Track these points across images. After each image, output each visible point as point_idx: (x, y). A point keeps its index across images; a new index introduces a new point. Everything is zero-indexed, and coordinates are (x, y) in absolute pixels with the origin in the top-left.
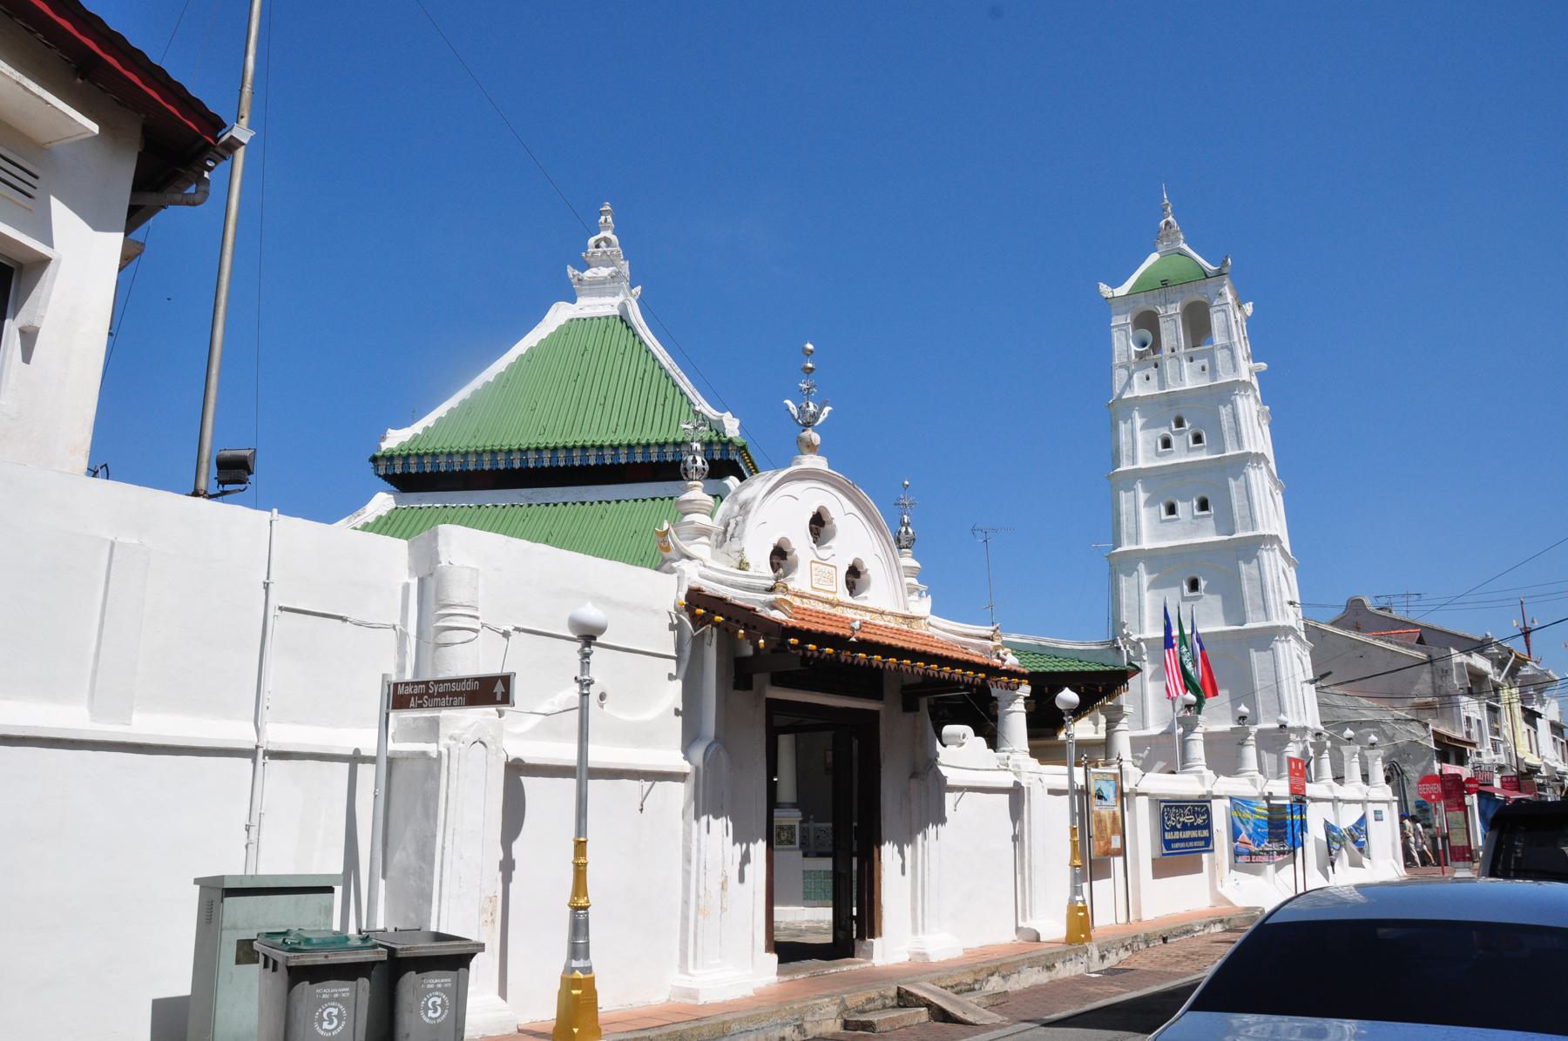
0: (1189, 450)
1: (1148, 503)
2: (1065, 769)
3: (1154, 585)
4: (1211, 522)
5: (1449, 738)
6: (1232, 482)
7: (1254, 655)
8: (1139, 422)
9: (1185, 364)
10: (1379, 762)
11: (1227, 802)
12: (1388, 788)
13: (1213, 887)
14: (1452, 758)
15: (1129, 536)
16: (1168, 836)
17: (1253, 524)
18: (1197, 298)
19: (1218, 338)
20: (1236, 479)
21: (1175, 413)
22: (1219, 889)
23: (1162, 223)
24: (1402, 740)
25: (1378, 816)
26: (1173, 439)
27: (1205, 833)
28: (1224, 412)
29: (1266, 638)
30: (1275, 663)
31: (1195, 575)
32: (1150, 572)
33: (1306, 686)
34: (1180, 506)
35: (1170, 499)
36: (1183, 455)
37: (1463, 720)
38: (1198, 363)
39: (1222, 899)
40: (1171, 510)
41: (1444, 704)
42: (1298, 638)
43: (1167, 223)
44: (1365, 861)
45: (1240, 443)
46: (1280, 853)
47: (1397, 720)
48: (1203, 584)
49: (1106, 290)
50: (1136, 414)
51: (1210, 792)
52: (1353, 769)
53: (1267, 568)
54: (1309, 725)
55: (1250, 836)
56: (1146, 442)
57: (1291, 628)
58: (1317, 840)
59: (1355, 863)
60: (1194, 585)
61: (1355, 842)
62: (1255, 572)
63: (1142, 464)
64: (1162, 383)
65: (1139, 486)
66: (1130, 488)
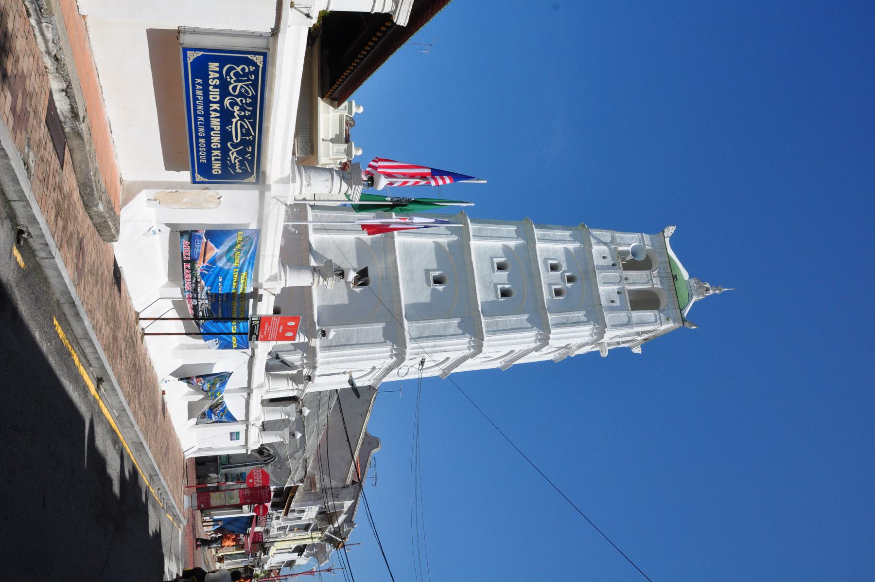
0: (550, 285)
1: (506, 249)
3: (438, 247)
4: (492, 298)
5: (293, 497)
6: (525, 317)
7: (380, 326)
8: (571, 246)
9: (616, 288)
10: (279, 440)
11: (253, 226)
12: (257, 447)
13: (148, 185)
14: (277, 500)
15: (480, 230)
16: (214, 66)
18: (664, 303)
19: (636, 315)
20: (528, 320)
21: (579, 275)
22: (143, 195)
23: (707, 285)
24: (291, 464)
25: (234, 436)
26: (557, 274)
27: (217, 167)
28: (581, 315)
29: (395, 337)
30: (373, 344)
31: (448, 282)
32: (450, 244)
33: (347, 377)
34: (504, 274)
35: (510, 266)
36: (546, 278)
37: (303, 508)
38: (616, 297)
39: (131, 192)
40: (501, 267)
41: (314, 494)
42: (389, 369)
43: (708, 289)
44: (194, 421)
45: (559, 325)
46: (195, 308)
47: (306, 461)
48: (440, 288)
50: (577, 245)
51: (268, 188)
52: (276, 414)
53: (455, 341)
55: (213, 262)
56: (555, 251)
57: (403, 360)
58: (212, 365)
59: (191, 407)
60: (438, 281)
61: (212, 409)
62: (451, 331)
63: (539, 246)
64: (603, 268)
65: (521, 242)
66: (519, 234)
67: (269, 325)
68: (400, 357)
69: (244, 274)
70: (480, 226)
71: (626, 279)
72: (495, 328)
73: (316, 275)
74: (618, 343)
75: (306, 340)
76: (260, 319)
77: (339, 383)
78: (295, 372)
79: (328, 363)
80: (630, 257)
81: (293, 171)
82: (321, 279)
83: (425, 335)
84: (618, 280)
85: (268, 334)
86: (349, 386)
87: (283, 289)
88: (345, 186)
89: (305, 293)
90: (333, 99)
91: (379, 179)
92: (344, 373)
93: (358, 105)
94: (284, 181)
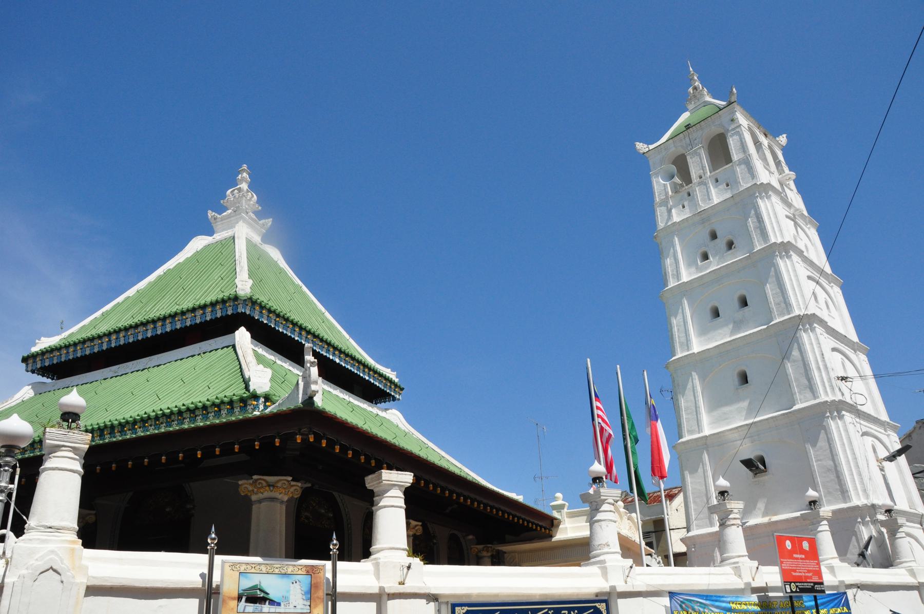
2: (204, 558)
11: (666, 601)
15: (681, 344)
17: (788, 306)
19: (736, 156)
33: (887, 464)
43: (695, 88)
49: (641, 147)
54: (876, 502)
63: (685, 277)
67: (795, 571)
68: (839, 408)
69: (733, 606)
70: (677, 346)
71: (701, 177)
72: (783, 305)
73: (728, 523)
74: (778, 164)
75: (825, 522)
76: (786, 582)
77: (900, 471)
78: (884, 530)
79: (865, 491)
80: (677, 180)
81: (594, 563)
82: (731, 516)
83: (806, 382)
84: (703, 187)
85: (809, 571)
86: (902, 459)
87: (752, 557)
88: (605, 507)
89: (750, 534)
90: (552, 525)
91: (594, 472)
92: (882, 470)
93: (555, 499)
94: (605, 572)
